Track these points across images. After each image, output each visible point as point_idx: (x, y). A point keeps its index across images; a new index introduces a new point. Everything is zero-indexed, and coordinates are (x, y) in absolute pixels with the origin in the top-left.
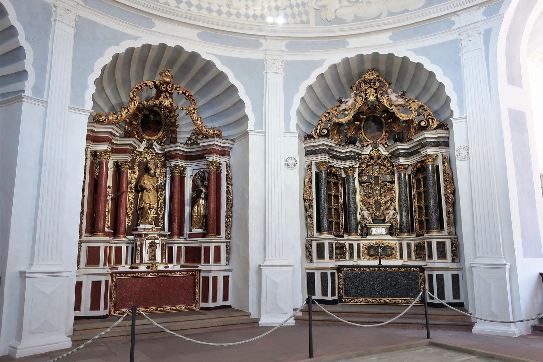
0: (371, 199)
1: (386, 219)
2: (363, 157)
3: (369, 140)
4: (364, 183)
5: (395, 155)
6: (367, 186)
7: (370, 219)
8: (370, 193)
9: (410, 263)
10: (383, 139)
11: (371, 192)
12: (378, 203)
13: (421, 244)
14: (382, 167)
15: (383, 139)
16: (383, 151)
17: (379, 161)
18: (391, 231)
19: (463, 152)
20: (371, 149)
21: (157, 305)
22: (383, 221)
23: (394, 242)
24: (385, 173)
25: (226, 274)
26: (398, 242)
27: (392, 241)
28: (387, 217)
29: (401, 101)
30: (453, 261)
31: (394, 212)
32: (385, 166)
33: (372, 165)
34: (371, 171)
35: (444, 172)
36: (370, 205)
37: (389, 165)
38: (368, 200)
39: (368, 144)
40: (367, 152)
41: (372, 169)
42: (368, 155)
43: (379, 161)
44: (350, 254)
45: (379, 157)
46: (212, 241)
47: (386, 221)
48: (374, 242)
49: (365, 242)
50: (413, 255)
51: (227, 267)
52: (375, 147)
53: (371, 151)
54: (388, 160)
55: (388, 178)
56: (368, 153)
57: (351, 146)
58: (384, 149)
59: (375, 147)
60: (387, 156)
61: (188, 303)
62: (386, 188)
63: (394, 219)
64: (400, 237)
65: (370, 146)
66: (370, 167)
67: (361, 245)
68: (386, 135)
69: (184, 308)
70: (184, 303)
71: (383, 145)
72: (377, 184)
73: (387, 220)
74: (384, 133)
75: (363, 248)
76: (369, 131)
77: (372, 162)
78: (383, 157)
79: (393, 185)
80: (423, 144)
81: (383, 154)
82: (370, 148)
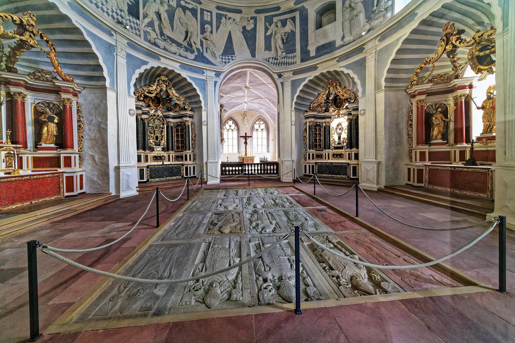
2: (151, 114)
5: (167, 117)
7: (153, 144)
9: (173, 163)
12: (157, 138)
16: (159, 113)
18: (163, 149)
19: (205, 123)
21: (31, 200)
22: (159, 145)
25: (81, 173)
27: (165, 154)
29: (177, 95)
30: (193, 161)
32: (160, 120)
35: (192, 128)
40: (152, 112)
45: (158, 116)
46: (63, 154)
50: (174, 159)
51: (81, 169)
52: (156, 111)
55: (162, 126)
59: (156, 111)
61: (55, 195)
66: (153, 120)
69: (53, 198)
70: (52, 196)
72: (156, 128)
76: (154, 102)
78: (160, 116)
79: (163, 130)
80: (186, 116)
82: (154, 111)
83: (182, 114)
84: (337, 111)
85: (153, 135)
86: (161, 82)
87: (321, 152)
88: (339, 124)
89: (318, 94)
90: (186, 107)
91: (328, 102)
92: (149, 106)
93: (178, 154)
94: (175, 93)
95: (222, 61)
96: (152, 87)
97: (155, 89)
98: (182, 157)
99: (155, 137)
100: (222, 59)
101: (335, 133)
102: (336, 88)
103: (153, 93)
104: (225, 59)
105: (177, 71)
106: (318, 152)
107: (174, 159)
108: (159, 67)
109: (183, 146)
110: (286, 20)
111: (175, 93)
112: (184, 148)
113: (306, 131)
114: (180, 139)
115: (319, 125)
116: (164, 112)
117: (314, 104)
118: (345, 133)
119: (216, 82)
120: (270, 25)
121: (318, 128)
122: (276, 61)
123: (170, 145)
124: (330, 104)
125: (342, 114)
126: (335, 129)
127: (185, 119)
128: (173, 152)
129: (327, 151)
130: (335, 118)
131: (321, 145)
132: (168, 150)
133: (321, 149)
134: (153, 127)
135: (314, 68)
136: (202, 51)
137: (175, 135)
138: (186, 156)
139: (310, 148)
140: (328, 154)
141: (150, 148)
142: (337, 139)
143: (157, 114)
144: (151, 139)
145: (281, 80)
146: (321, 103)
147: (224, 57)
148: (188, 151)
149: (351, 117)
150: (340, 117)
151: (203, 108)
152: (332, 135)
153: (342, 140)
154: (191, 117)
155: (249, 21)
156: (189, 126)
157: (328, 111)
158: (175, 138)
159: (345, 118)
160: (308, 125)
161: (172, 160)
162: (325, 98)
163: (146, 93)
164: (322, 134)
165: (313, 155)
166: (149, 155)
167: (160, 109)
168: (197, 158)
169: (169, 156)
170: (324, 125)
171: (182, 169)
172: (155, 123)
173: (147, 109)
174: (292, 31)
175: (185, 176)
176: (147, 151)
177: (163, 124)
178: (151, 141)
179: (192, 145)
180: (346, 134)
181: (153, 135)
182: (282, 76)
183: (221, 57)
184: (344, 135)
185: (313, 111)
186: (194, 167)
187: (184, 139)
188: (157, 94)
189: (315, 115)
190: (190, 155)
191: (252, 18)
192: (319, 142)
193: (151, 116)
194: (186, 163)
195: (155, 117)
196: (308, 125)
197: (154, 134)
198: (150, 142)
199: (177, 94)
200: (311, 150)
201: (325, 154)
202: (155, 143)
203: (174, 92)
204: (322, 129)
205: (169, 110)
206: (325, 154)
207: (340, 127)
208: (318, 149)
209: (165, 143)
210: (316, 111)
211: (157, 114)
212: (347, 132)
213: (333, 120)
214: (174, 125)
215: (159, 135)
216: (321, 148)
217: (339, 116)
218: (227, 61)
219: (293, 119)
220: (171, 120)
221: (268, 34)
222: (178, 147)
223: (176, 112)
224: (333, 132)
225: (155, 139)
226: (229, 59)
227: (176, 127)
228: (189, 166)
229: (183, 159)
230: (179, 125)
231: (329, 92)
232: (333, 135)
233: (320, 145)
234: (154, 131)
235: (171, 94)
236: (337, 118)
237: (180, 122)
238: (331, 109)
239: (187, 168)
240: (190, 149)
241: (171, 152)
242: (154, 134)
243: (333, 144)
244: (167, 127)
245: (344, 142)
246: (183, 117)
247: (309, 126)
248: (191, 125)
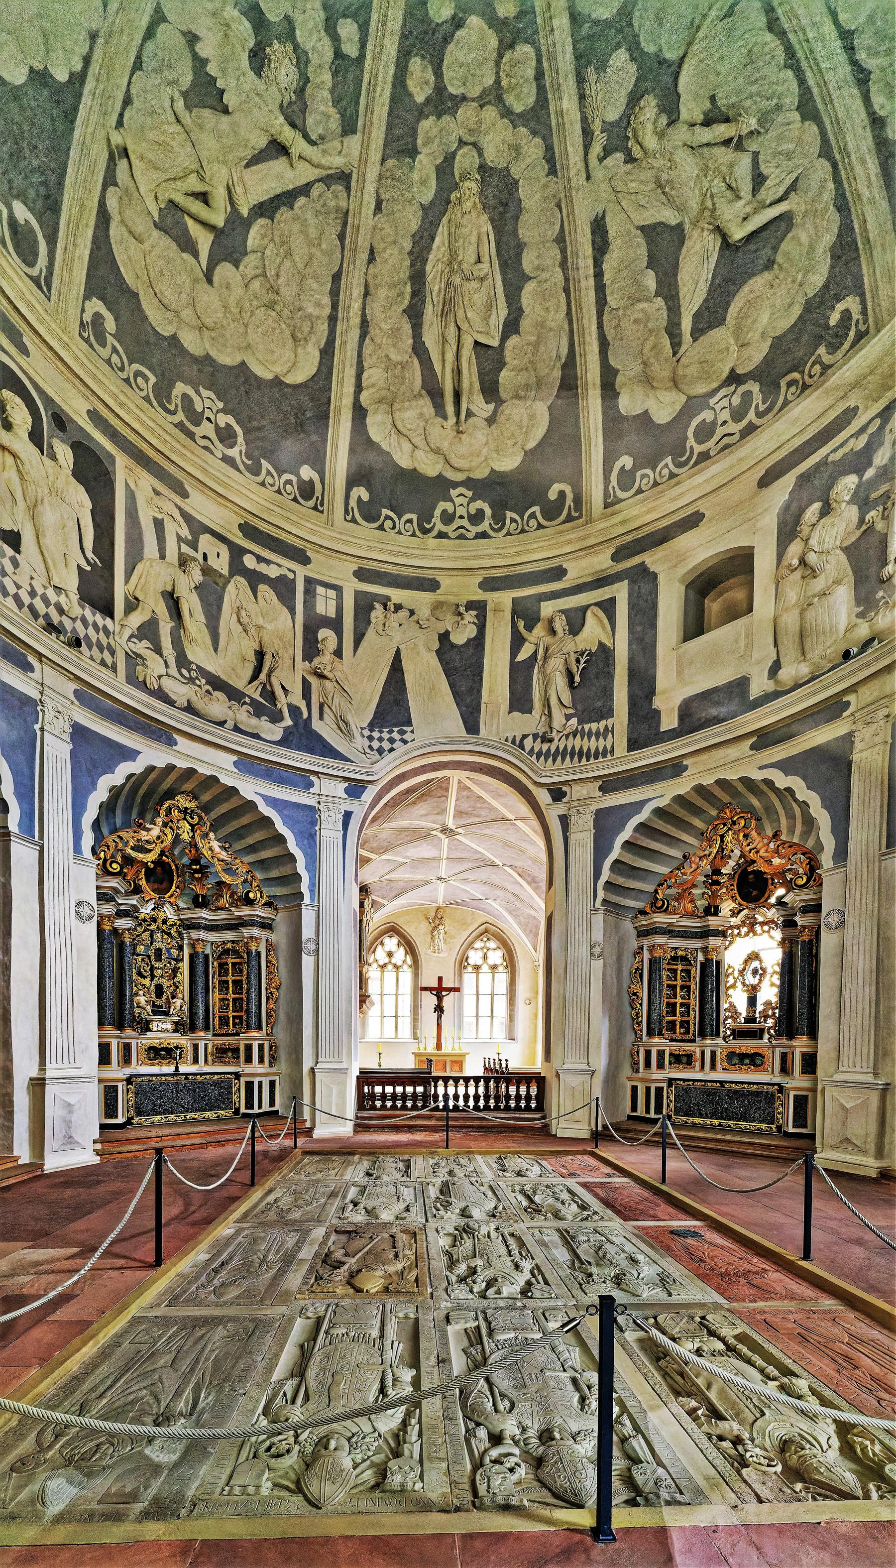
2: (142, 916)
7: (149, 1008)
10: (171, 896)
15: (171, 896)
17: (164, 927)
18: (178, 1027)
27: (185, 1042)
30: (271, 1065)
32: (169, 934)
43: (164, 927)
45: (164, 922)
52: (158, 907)
55: (175, 953)
57: (136, 897)
59: (158, 907)
64: (193, 1036)
76: (152, 879)
78: (170, 922)
82: (151, 905)
83: (240, 917)
84: (745, 912)
85: (147, 982)
86: (175, 813)
87: (688, 1047)
88: (754, 956)
89: (684, 856)
90: (251, 895)
91: (717, 883)
92: (137, 891)
93: (220, 1041)
94: (217, 849)
95: (370, 747)
96: (148, 830)
97: (158, 838)
98: (236, 1051)
99: (153, 988)
100: (371, 738)
101: (739, 984)
102: (746, 836)
103: (150, 851)
104: (380, 739)
105: (227, 780)
106: (677, 1047)
107: (210, 1058)
108: (171, 768)
109: (240, 1018)
110: (584, 609)
111: (217, 849)
113: (641, 976)
114: (231, 996)
115: (684, 959)
116: (183, 909)
117: (669, 887)
118: (773, 985)
119: (348, 815)
120: (530, 628)
121: (680, 967)
122: (545, 747)
123: (200, 1013)
124: (724, 890)
125: (762, 924)
126: (736, 974)
127: (247, 932)
128: (209, 1035)
129: (708, 1042)
130: (739, 934)
131: (688, 1022)
132: (193, 1028)
133: (690, 1037)
134: (149, 957)
135: (675, 768)
136: (305, 716)
137: (214, 981)
138: (249, 1048)
139: (650, 1033)
140: (713, 1054)
142: (742, 1007)
143: (161, 916)
144: (141, 993)
145: (560, 809)
146: (694, 886)
147: (376, 734)
148: (254, 1034)
149: (791, 931)
150: (755, 934)
151: (307, 899)
152: (728, 989)
153: (760, 1007)
154: (266, 926)
155: (460, 614)
156: (259, 954)
157: (716, 914)
159: (771, 937)
160: (646, 955)
161: (206, 1061)
162: (708, 869)
163: (129, 851)
164: (695, 986)
165: (661, 1054)
166: (134, 1043)
167: (172, 900)
168: (283, 1055)
169: (195, 1048)
170: (701, 957)
171: (234, 1089)
172: (156, 945)
173: (132, 901)
174: (601, 645)
175: (243, 1110)
176: (129, 1032)
177: (180, 948)
178: (142, 1000)
179: (269, 1016)
180: (776, 990)
181: (147, 982)
182: (564, 794)
183: (366, 733)
184: (769, 993)
185: (666, 911)
186: (272, 1084)
187: (244, 996)
188: (162, 853)
189: (670, 924)
190: (261, 1047)
191: (470, 606)
192: (681, 1014)
194: (248, 1069)
195: (154, 926)
196: (646, 955)
197: (152, 980)
198: (138, 1003)
199: (224, 853)
200: (656, 1040)
201: (703, 1053)
202: (154, 1005)
203: (216, 845)
204: (696, 973)
205: (199, 902)
206: (703, 1053)
207: (755, 964)
208: (678, 1037)
209: (186, 1008)
210: (674, 913)
211: (161, 916)
212: (778, 982)
213: (731, 943)
214: (213, 952)
215: (165, 983)
216: (687, 1032)
217: (752, 930)
218: (386, 745)
219: (598, 935)
220: (202, 934)
221: (521, 657)
222: (224, 1021)
223: (219, 909)
224: (731, 980)
225: (153, 995)
226: (392, 741)
227: (219, 957)
228: (256, 1081)
229: (238, 1057)
230: (228, 950)
231: (721, 849)
232: (731, 992)
233: (685, 1025)
235: (207, 853)
236: (747, 934)
237: (233, 942)
238: (727, 906)
239: (249, 1086)
240: (260, 1028)
241: (202, 1034)
242: (152, 980)
243: (730, 1021)
244: (193, 957)
245: (766, 1017)
246: (242, 925)
247: (650, 961)
248: (268, 950)
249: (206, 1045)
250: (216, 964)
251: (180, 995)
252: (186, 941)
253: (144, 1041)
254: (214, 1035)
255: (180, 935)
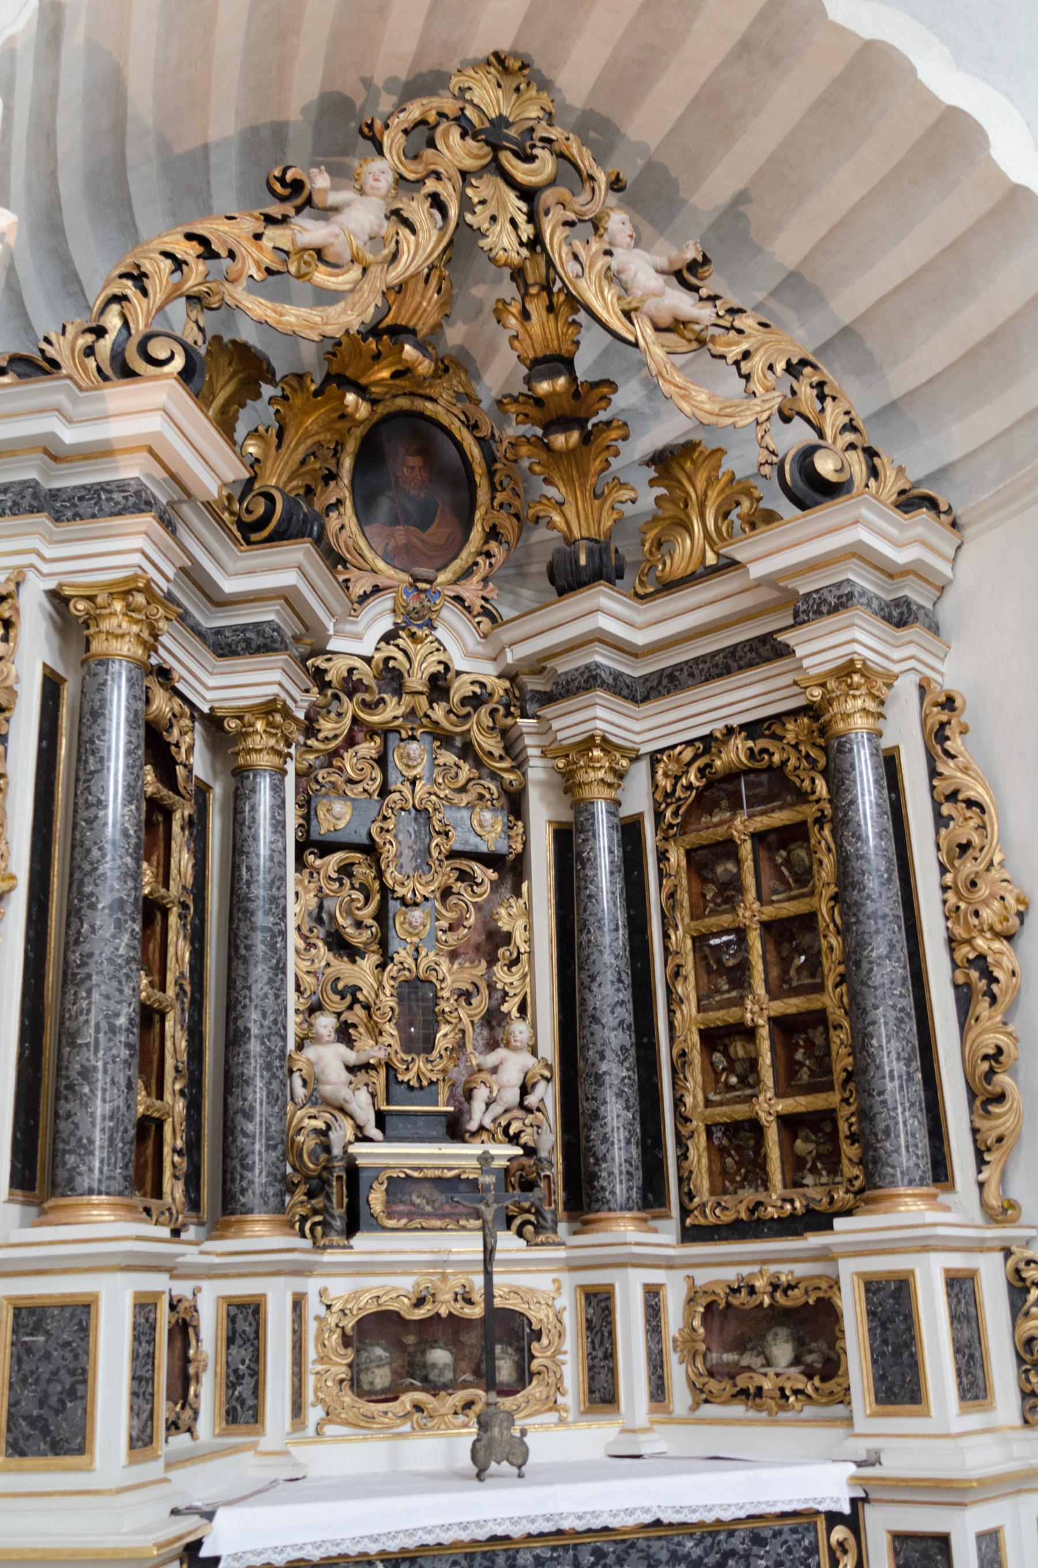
0: (368, 963)
1: (478, 1105)
3: (380, 564)
4: (326, 848)
6: (346, 870)
8: (359, 924)
10: (467, 573)
11: (367, 914)
13: (752, 1290)
14: (448, 757)
15: (467, 573)
17: (439, 712)
20: (386, 624)
23: (542, 1282)
24: (465, 799)
26: (570, 1281)
28: (481, 1095)
31: (529, 1061)
33: (385, 732)
34: (377, 773)
36: (357, 1008)
37: (490, 744)
38: (342, 967)
39: (377, 590)
41: (382, 761)
42: (368, 660)
44: (231, 1386)
47: (473, 1126)
48: (407, 1283)
49: (339, 1288)
53: (388, 637)
54: (493, 712)
56: (366, 647)
58: (471, 639)
60: (491, 681)
62: (467, 897)
63: (529, 1110)
65: (383, 603)
66: (368, 748)
67: (314, 1308)
68: (488, 555)
71: (468, 609)
73: (478, 1115)
74: (476, 535)
75: (320, 1332)
77: (392, 710)
78: (460, 689)
81: (459, 673)
90: (826, 466)
99: (388, 1001)
107: (677, 1373)
112: (832, 1161)
141: (317, 1187)
158: (687, 989)
161: (658, 1390)
167: (470, 590)
193: (351, 686)
214: (662, 799)
230: (732, 776)
234: (382, 916)
237: (752, 729)
248: (938, 735)
249: (653, 1294)
250: (676, 857)
251: (520, 1030)
252: (537, 771)
253: (339, 1288)
254: (690, 1234)
255: (512, 748)
